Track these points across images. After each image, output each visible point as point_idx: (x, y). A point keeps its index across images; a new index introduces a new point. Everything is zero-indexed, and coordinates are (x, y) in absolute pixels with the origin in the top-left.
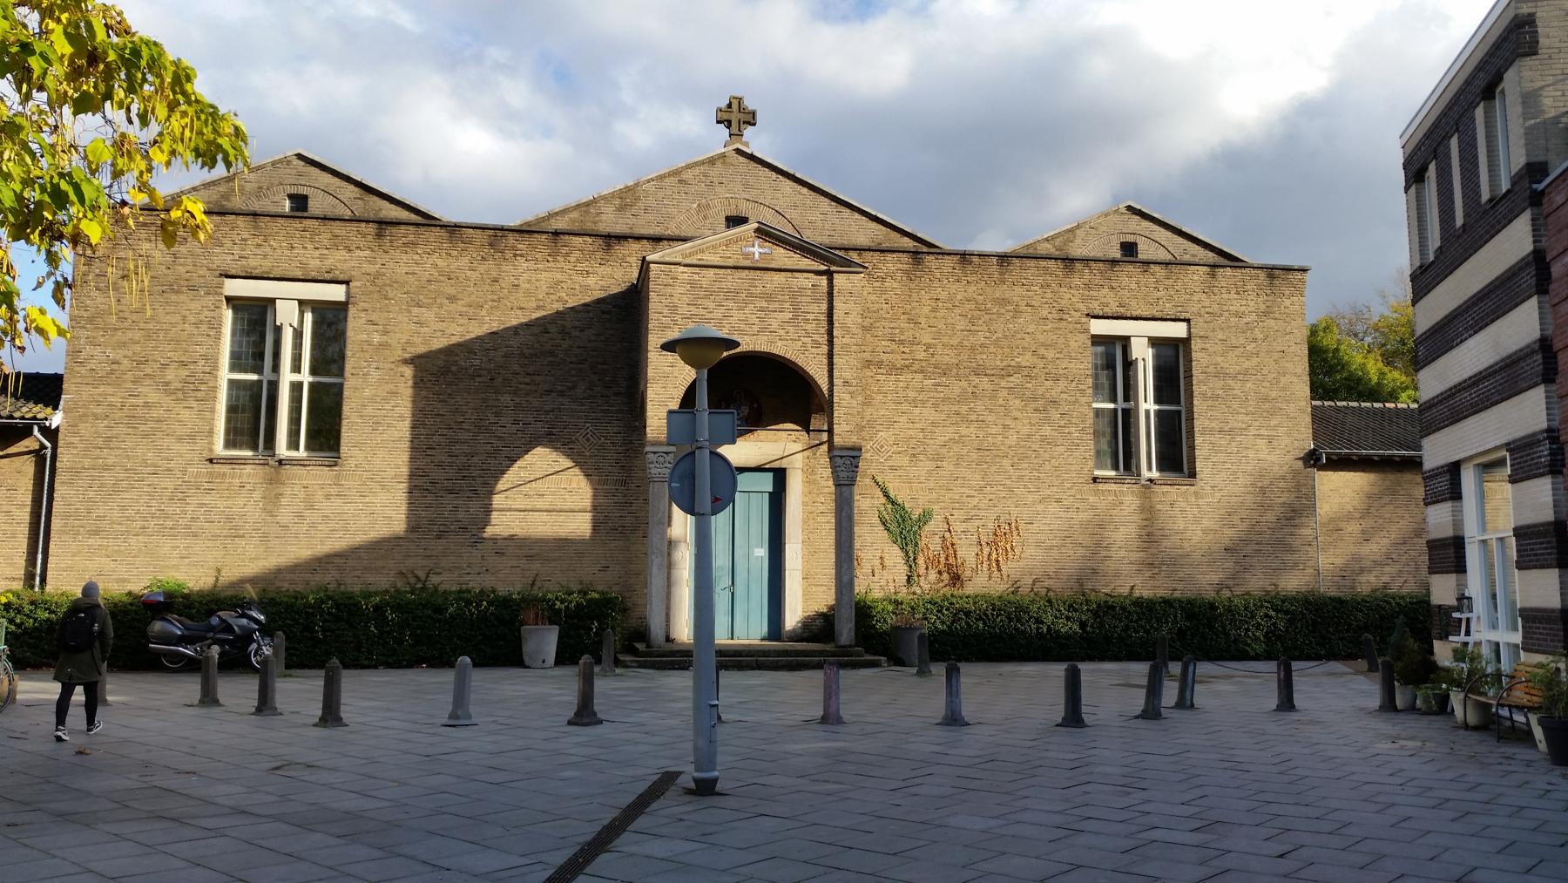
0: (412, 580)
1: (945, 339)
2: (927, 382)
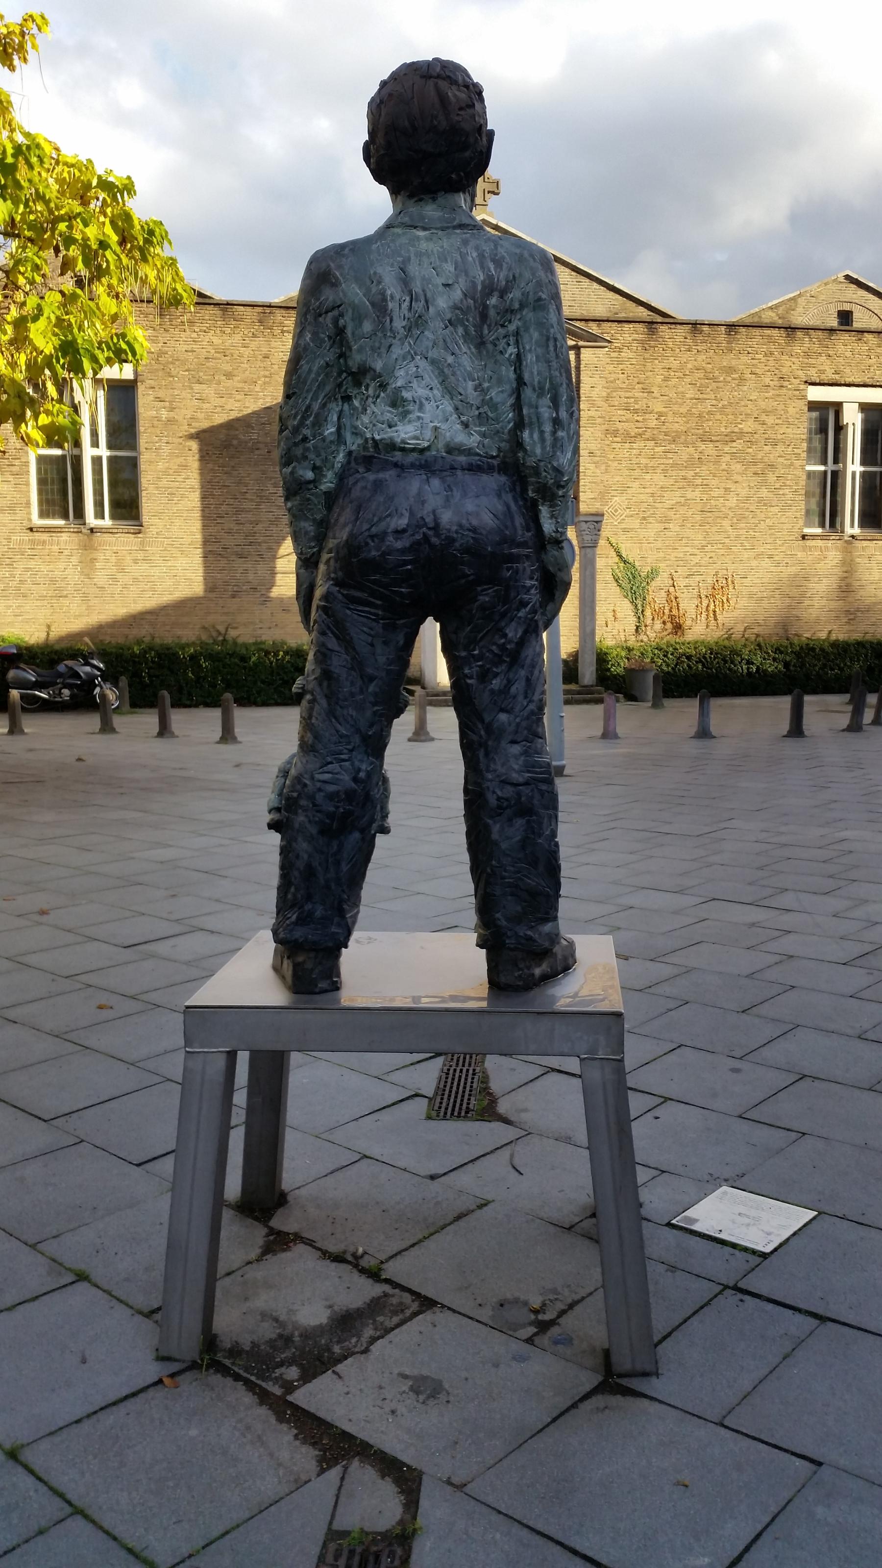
0: (214, 634)
1: (675, 408)
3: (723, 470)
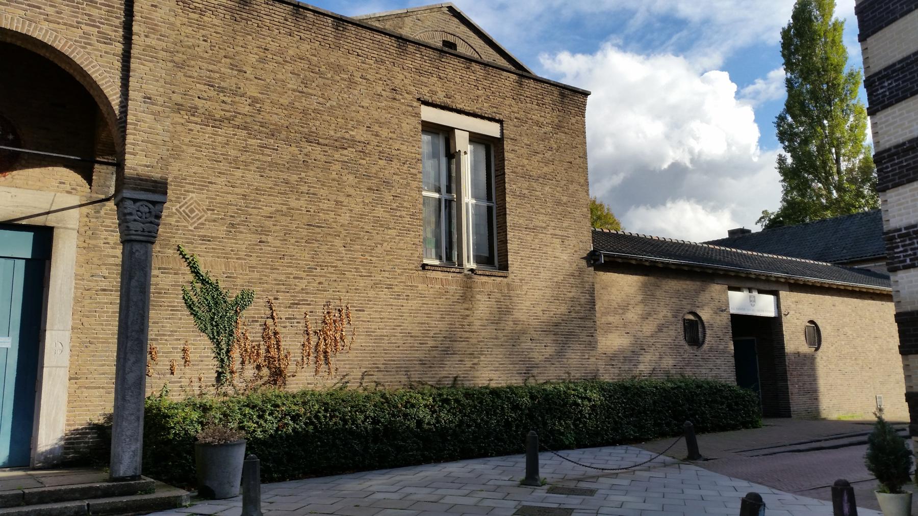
1: (274, 96)
2: (251, 141)
3: (333, 180)
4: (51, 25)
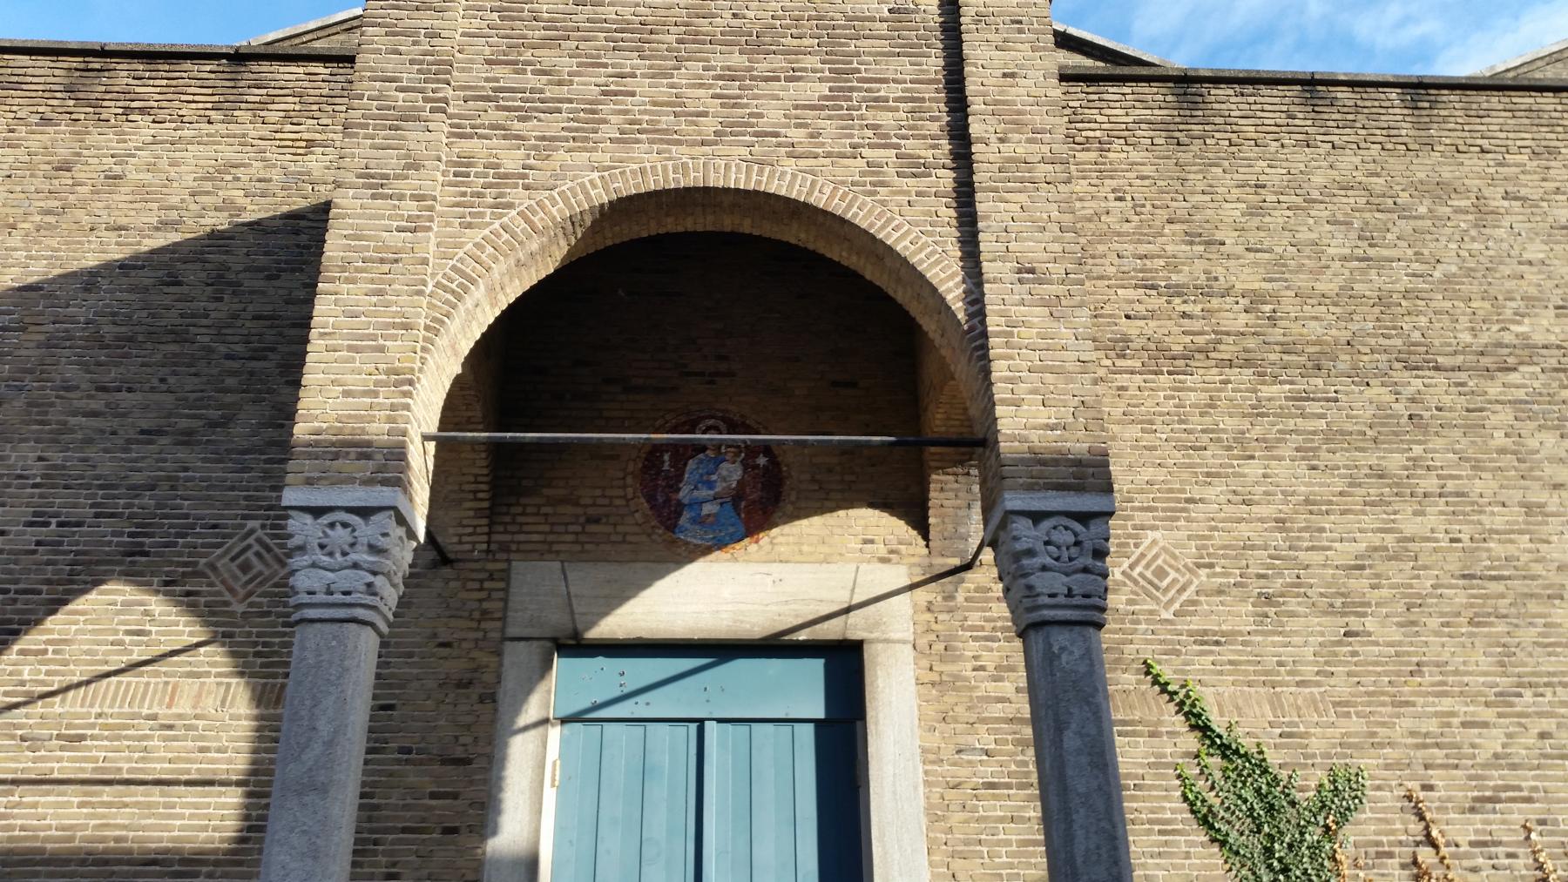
1: (1302, 281)
2: (1267, 391)
3: (1502, 451)
4: (803, 163)
